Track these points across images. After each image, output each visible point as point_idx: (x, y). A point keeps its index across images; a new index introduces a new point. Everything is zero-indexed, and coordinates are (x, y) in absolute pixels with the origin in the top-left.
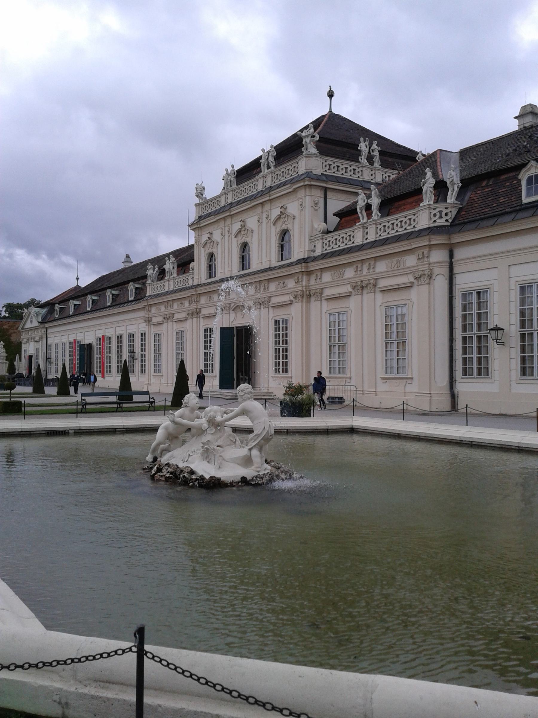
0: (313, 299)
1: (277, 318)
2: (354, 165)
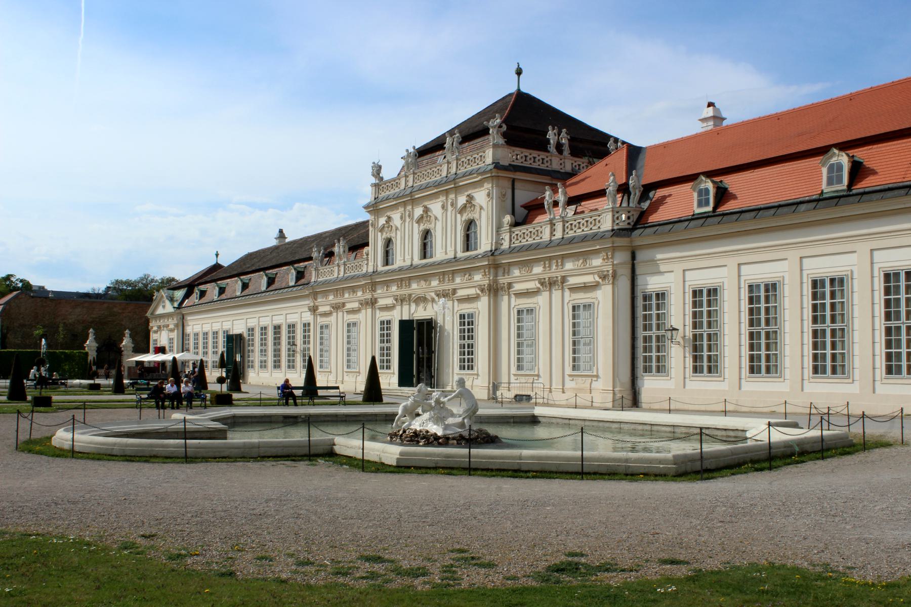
0: (500, 293)
1: (462, 312)
2: (543, 155)
